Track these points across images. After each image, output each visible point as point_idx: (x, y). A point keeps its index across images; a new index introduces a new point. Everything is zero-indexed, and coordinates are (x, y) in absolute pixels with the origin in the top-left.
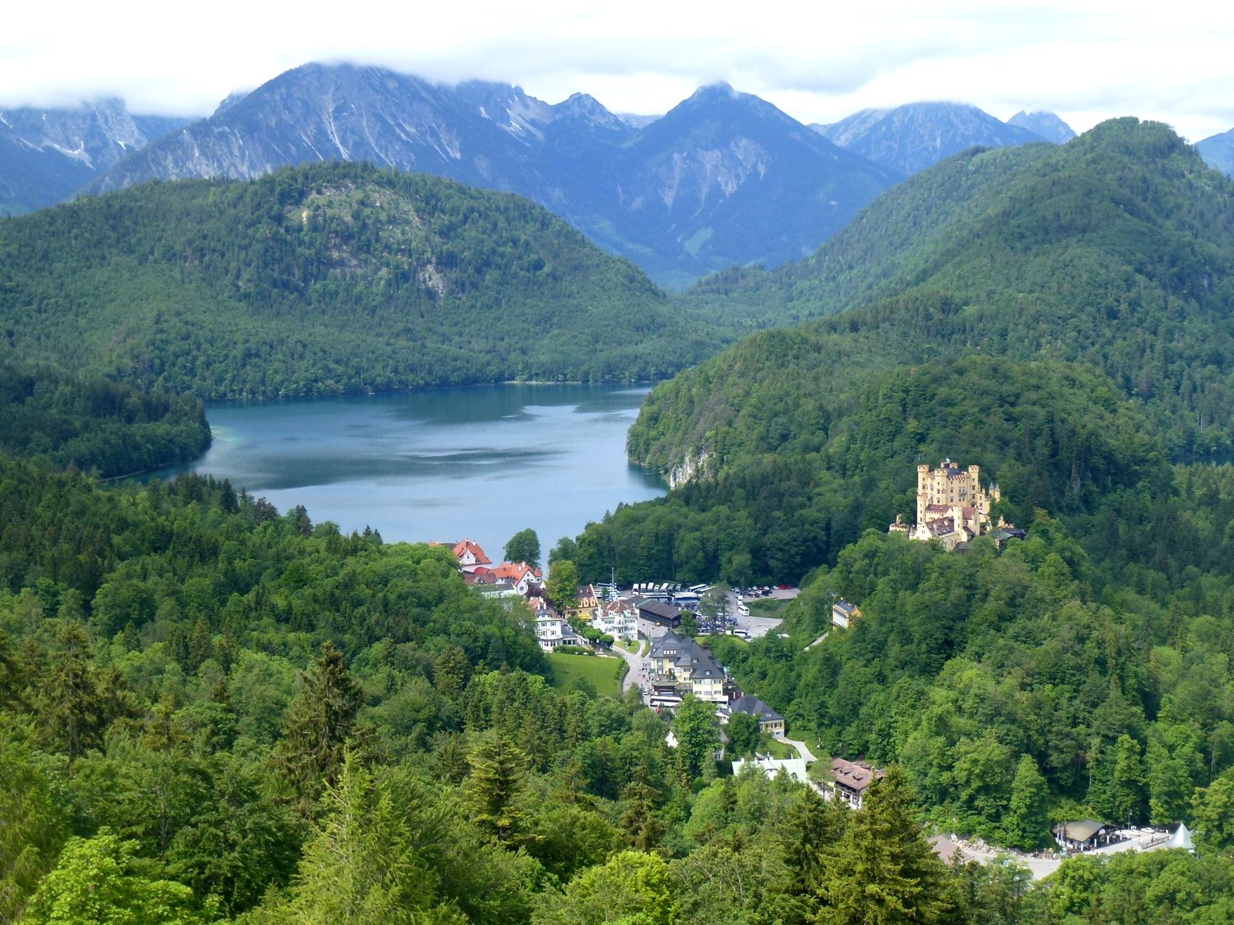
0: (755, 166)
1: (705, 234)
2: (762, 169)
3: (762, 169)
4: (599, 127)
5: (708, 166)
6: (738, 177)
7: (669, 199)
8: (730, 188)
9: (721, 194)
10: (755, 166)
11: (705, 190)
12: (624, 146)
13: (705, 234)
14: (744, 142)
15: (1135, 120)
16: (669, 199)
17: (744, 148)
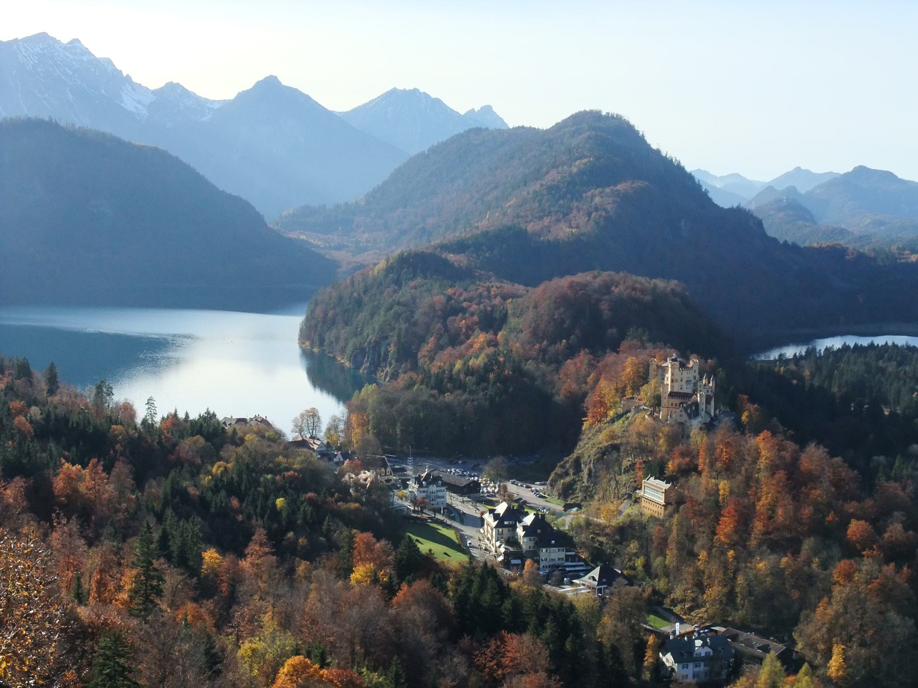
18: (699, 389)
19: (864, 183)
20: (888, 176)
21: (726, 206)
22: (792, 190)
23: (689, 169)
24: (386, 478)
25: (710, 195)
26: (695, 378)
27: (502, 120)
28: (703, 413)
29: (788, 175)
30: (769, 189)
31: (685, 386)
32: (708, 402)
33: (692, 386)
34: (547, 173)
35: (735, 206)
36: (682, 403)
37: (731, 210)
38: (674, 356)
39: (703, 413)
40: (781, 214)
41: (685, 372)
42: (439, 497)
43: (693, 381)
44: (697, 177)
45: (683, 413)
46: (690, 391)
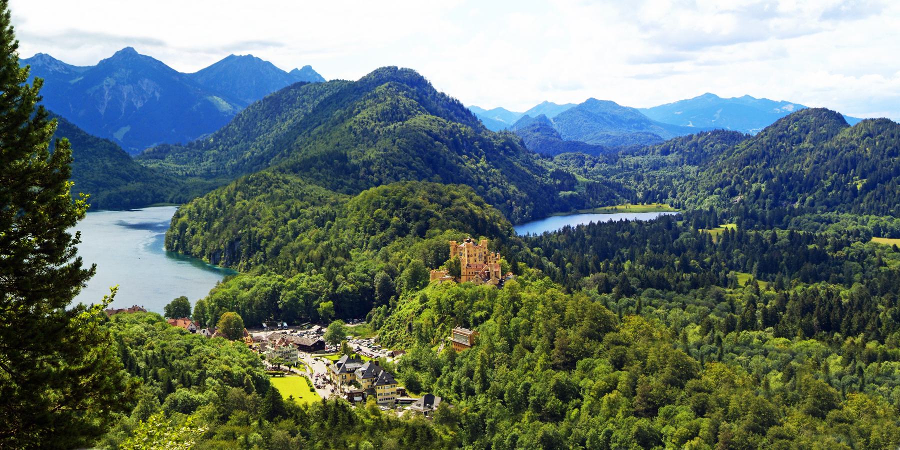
0: (153, 93)
1: (125, 130)
2: (158, 95)
3: (158, 95)
4: (55, 72)
5: (125, 94)
6: (143, 99)
7: (102, 111)
8: (139, 105)
9: (135, 109)
10: (153, 93)
11: (124, 105)
12: (73, 82)
13: (125, 130)
14: (146, 81)
15: (396, 68)
16: (102, 111)
17: (146, 84)
19: (593, 110)
20: (612, 104)
22: (543, 118)
23: (466, 106)
27: (320, 76)
28: (494, 278)
29: (538, 107)
30: (526, 117)
34: (359, 112)
38: (468, 238)
40: (536, 134)
44: (473, 111)
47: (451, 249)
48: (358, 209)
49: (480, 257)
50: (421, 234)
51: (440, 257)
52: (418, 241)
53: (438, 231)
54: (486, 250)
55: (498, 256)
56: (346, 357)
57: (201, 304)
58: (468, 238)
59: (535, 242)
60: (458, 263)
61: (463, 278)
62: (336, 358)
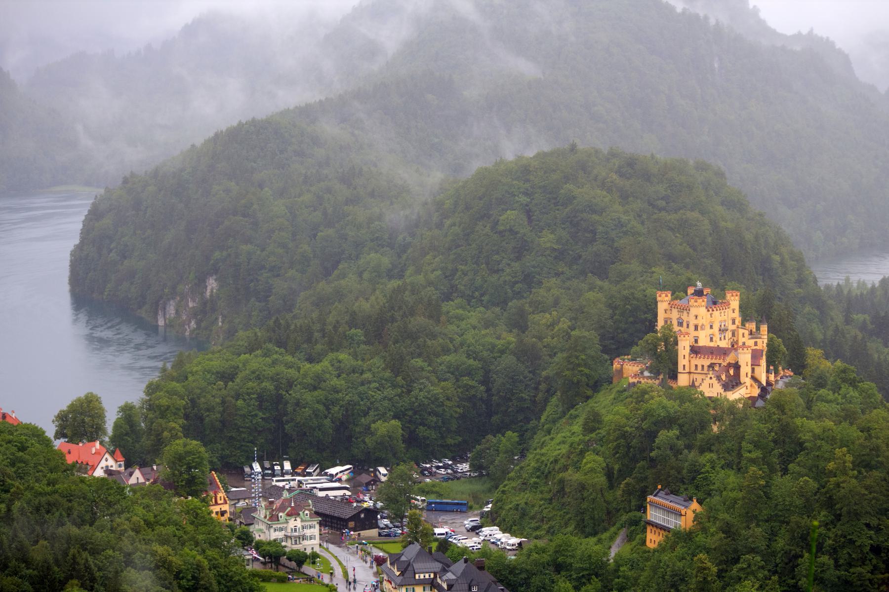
18: (741, 340)
21: (790, 33)
24: (216, 509)
25: (763, 15)
26: (734, 323)
28: (748, 381)
31: (717, 336)
32: (755, 363)
33: (729, 335)
35: (805, 32)
36: (711, 366)
37: (798, 37)
39: (746, 380)
41: (716, 313)
42: (304, 538)
43: (732, 327)
45: (714, 381)
46: (724, 344)
47: (662, 307)
48: (468, 208)
49: (722, 331)
50: (601, 271)
51: (634, 329)
52: (591, 288)
53: (635, 266)
54: (737, 315)
55: (764, 328)
56: (416, 547)
57: (127, 411)
58: (699, 284)
59: (853, 302)
60: (671, 343)
61: (683, 380)
62: (396, 549)
